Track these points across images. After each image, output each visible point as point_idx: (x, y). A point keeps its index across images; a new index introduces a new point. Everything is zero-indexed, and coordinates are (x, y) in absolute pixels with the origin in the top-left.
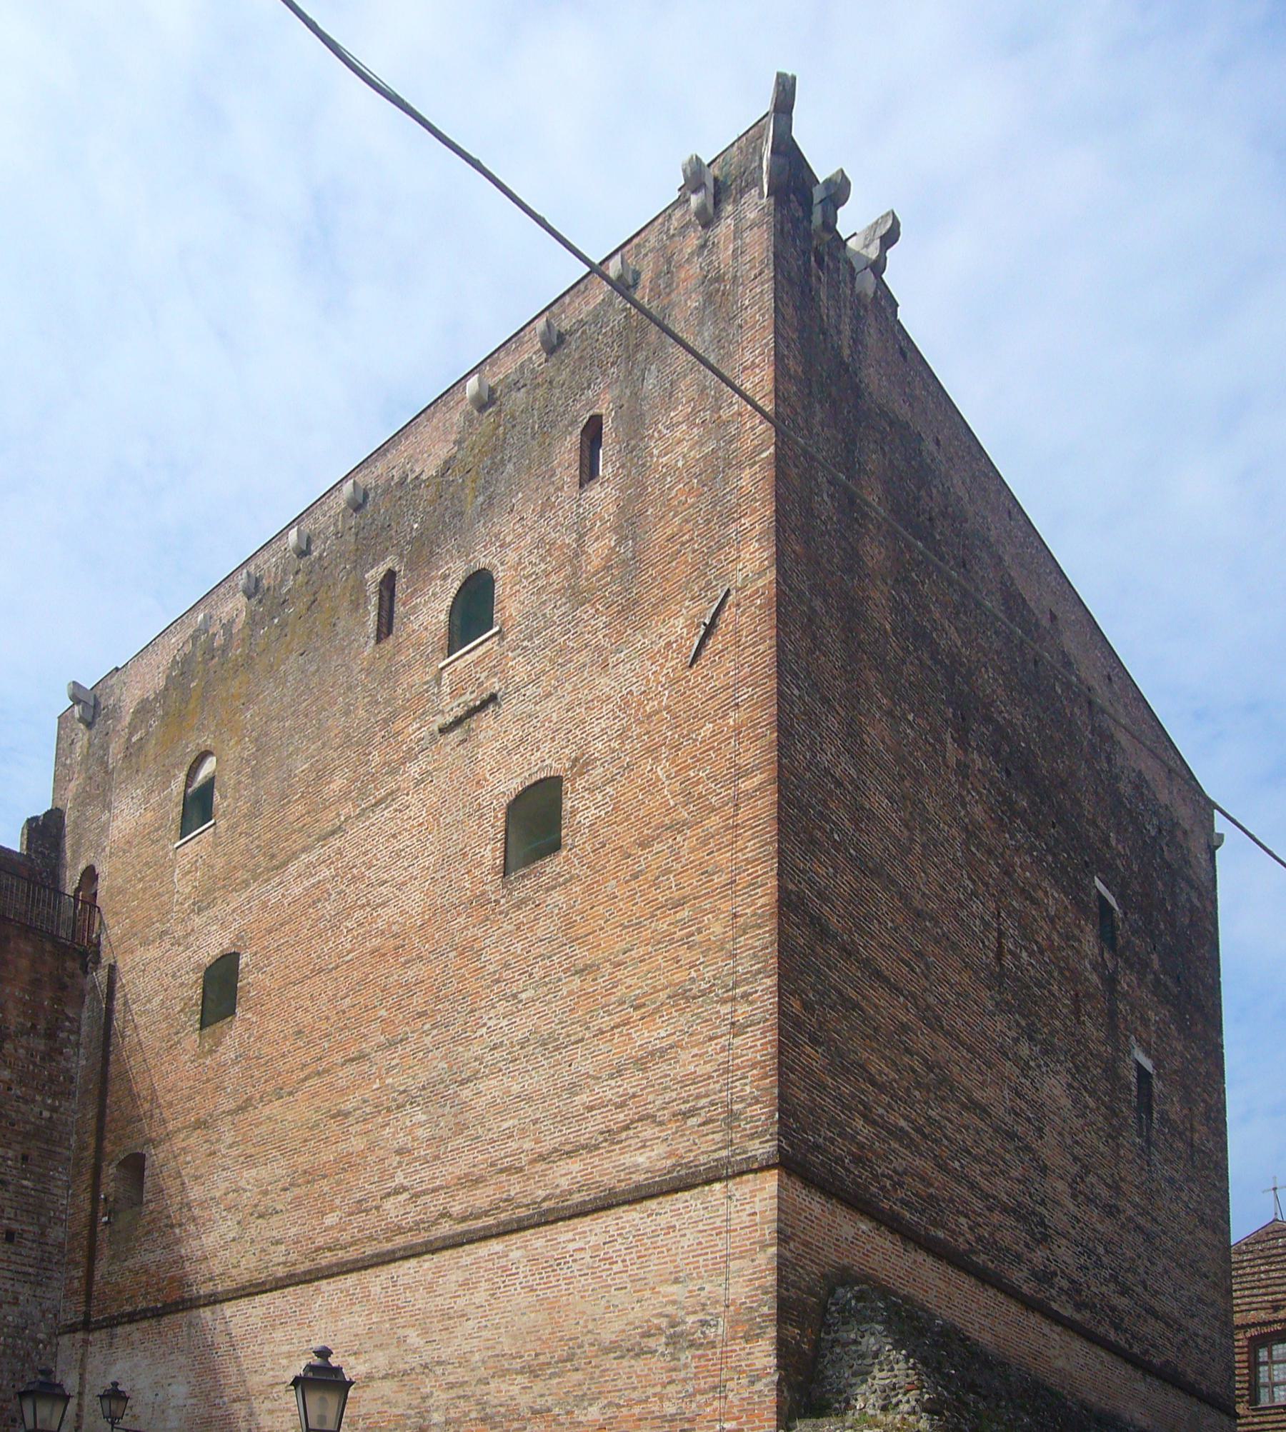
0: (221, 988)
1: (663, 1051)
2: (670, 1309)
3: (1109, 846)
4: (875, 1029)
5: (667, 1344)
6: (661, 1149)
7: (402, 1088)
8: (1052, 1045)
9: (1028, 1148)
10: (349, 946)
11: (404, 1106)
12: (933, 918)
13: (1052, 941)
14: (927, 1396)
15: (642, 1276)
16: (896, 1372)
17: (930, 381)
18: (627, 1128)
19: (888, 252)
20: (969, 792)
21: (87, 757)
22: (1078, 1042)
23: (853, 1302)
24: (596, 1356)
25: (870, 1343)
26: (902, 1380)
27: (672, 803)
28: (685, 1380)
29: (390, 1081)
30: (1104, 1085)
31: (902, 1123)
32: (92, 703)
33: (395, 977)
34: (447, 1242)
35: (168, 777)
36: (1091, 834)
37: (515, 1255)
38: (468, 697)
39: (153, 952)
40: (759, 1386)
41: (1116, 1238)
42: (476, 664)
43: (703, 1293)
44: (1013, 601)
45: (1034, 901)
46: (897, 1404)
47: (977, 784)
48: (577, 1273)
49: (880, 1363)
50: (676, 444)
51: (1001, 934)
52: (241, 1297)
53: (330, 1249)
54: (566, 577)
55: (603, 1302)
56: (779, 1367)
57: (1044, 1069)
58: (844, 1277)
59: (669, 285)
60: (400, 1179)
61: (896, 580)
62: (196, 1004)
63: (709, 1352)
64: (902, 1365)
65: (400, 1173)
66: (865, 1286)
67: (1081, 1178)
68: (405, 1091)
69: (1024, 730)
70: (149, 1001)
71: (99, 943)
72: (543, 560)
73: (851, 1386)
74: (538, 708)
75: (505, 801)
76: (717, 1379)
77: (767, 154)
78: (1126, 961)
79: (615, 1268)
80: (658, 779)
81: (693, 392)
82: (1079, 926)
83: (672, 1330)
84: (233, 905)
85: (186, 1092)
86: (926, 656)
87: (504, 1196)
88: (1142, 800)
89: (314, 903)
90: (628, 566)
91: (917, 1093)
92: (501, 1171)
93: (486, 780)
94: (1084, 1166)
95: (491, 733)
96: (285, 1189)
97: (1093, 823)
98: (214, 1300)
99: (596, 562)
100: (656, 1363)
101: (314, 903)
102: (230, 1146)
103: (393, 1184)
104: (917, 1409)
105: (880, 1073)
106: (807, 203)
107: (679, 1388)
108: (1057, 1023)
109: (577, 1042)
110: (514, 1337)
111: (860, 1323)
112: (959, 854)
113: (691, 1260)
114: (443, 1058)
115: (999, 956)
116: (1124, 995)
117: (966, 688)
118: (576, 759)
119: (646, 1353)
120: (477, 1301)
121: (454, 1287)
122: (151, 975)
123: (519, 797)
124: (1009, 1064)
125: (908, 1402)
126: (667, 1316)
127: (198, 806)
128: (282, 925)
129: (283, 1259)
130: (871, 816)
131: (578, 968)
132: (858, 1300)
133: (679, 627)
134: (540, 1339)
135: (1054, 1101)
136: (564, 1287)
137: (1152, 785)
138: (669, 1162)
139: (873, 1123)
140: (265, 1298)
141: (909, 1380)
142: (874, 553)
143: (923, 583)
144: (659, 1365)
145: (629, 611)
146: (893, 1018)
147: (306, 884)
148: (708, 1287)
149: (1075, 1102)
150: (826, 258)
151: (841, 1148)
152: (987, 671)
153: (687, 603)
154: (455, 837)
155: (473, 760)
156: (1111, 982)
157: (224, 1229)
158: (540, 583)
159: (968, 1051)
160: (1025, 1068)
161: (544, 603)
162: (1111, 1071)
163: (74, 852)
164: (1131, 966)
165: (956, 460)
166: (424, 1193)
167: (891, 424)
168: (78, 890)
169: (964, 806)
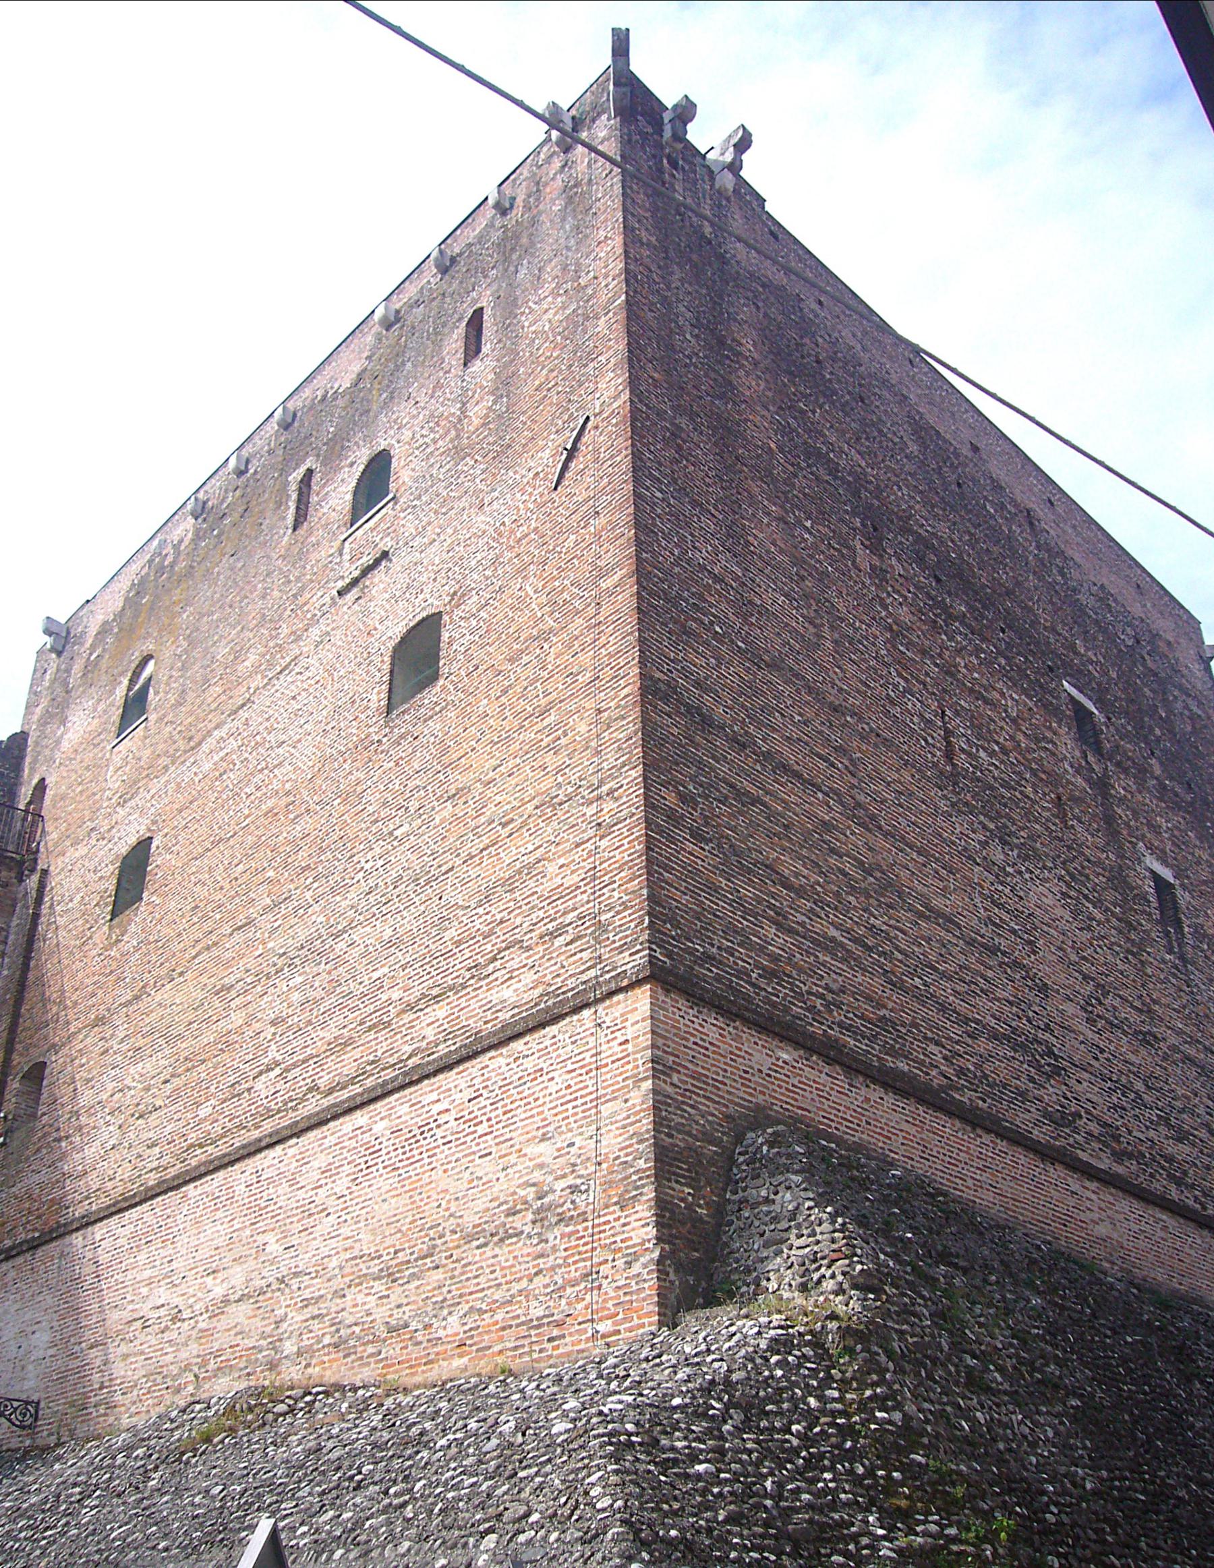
0: (134, 872)
1: (530, 867)
2: (537, 1176)
3: (1076, 653)
4: (786, 827)
5: (534, 1222)
6: (529, 977)
7: (282, 951)
8: (1034, 849)
9: (1016, 964)
10: (246, 812)
11: (282, 970)
12: (856, 714)
13: (1018, 743)
14: (859, 1267)
15: (508, 1136)
16: (819, 1237)
17: (807, 257)
18: (494, 959)
19: (744, 157)
20: (889, 595)
21: (53, 681)
22: (1069, 848)
23: (765, 1148)
24: (458, 1247)
25: (786, 1200)
26: (825, 1248)
27: (539, 615)
28: (553, 1268)
29: (271, 945)
30: (1110, 896)
31: (833, 932)
32: (64, 634)
33: (285, 835)
34: (312, 1122)
35: (115, 682)
36: (1052, 640)
37: (379, 1128)
38: (365, 559)
39: (82, 850)
40: (636, 1268)
41: (1158, 1072)
42: (372, 530)
43: (573, 1150)
44: (921, 430)
45: (986, 701)
46: (819, 1282)
47: (897, 587)
48: (440, 1141)
49: (799, 1226)
50: (543, 313)
51: (948, 733)
52: (112, 1214)
53: (201, 1146)
54: (452, 441)
55: (467, 1175)
56: (659, 1239)
57: (1027, 876)
58: (759, 1117)
59: (538, 200)
60: (273, 1054)
61: (780, 408)
62: (110, 896)
63: (580, 1227)
64: (826, 1227)
65: (274, 1047)
66: (781, 1128)
67: (1097, 999)
68: (284, 953)
69: (952, 541)
70: (71, 901)
71: (38, 851)
72: (432, 430)
73: (762, 1260)
74: (423, 555)
75: (391, 644)
76: (588, 1263)
77: (611, 87)
78: (1118, 764)
79: (481, 1129)
80: (527, 595)
81: (557, 271)
82: (1050, 728)
83: (539, 1203)
84: (153, 792)
85: (90, 989)
86: (822, 472)
87: (371, 1058)
88: (1110, 612)
89: (221, 775)
90: (501, 421)
91: (851, 898)
92: (370, 1029)
93: (375, 629)
94: (1098, 986)
95: (382, 586)
96: (166, 1082)
97: (1053, 629)
98: (88, 1222)
99: (477, 422)
100: (522, 1248)
101: (221, 775)
102: (122, 1041)
103: (266, 1061)
104: (845, 1286)
105: (797, 875)
106: (658, 125)
107: (547, 1280)
108: (1037, 827)
109: (447, 872)
110: (373, 1232)
111: (772, 1175)
112: (883, 652)
113: (560, 1109)
114: (322, 912)
115: (949, 755)
116: (1120, 799)
117: (876, 503)
118: (455, 593)
119: (511, 1236)
120: (337, 1190)
121: (316, 1175)
122: (76, 871)
123: (404, 640)
124: (977, 869)
125: (833, 1276)
126: (534, 1185)
127: (135, 706)
128: (191, 803)
129: (155, 1164)
130: (762, 611)
131: (450, 794)
132: (772, 1145)
133: (547, 458)
134: (400, 1231)
135: (1046, 911)
136: (427, 1161)
137: (1119, 598)
138: (537, 992)
139: (791, 931)
140: (133, 1213)
141: (834, 1246)
142: (751, 384)
143: (814, 412)
144: (526, 1251)
145: (503, 454)
146: (809, 815)
147: (216, 758)
148: (578, 1141)
149: (1075, 913)
150: (681, 162)
151: (743, 959)
152: (900, 489)
153: (552, 437)
154: (346, 688)
155: (366, 613)
156: (1102, 786)
157: (106, 1136)
158: (429, 450)
159: (919, 853)
160: (1000, 876)
161: (432, 466)
162: (1118, 879)
163: (31, 769)
164: (1125, 771)
165: (842, 317)
166: (295, 1065)
167: (764, 286)
168: (30, 803)
169: (885, 607)
